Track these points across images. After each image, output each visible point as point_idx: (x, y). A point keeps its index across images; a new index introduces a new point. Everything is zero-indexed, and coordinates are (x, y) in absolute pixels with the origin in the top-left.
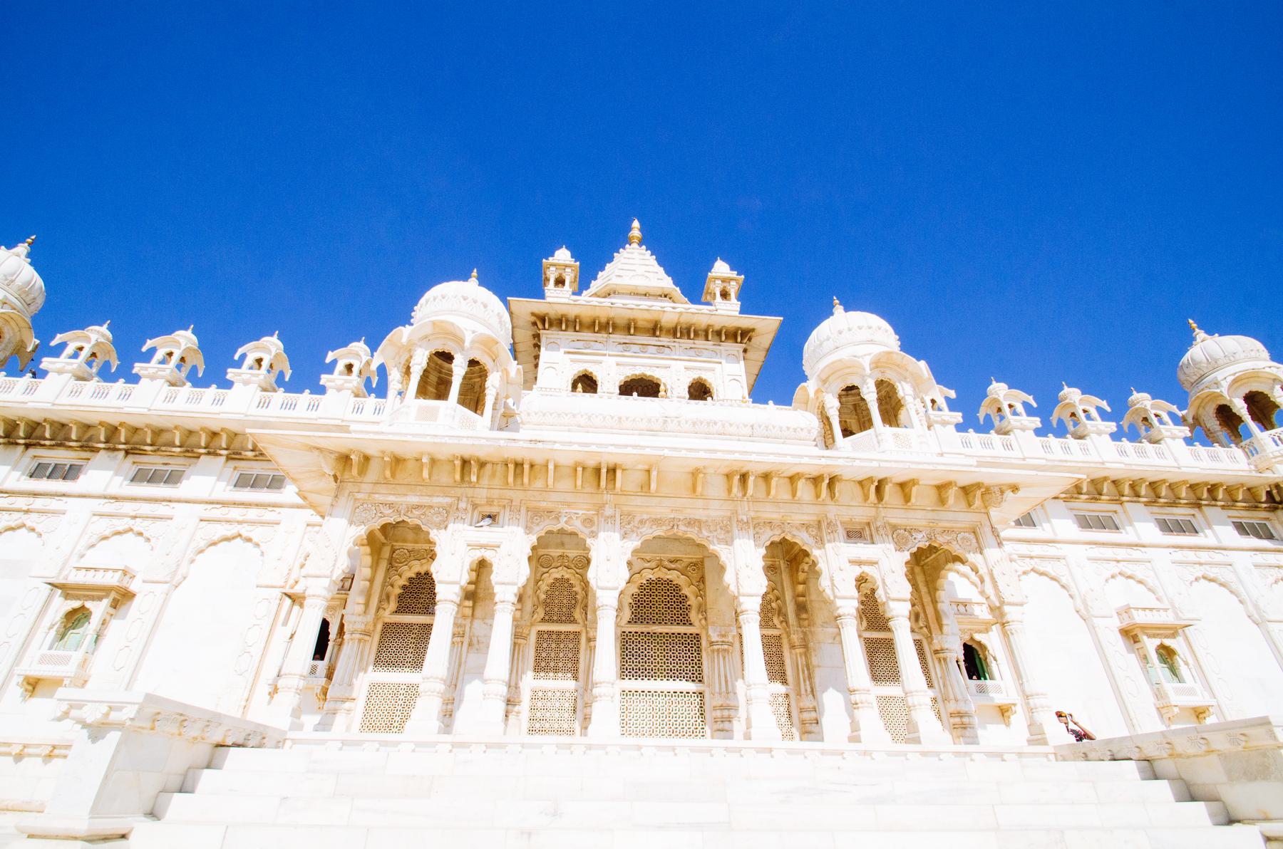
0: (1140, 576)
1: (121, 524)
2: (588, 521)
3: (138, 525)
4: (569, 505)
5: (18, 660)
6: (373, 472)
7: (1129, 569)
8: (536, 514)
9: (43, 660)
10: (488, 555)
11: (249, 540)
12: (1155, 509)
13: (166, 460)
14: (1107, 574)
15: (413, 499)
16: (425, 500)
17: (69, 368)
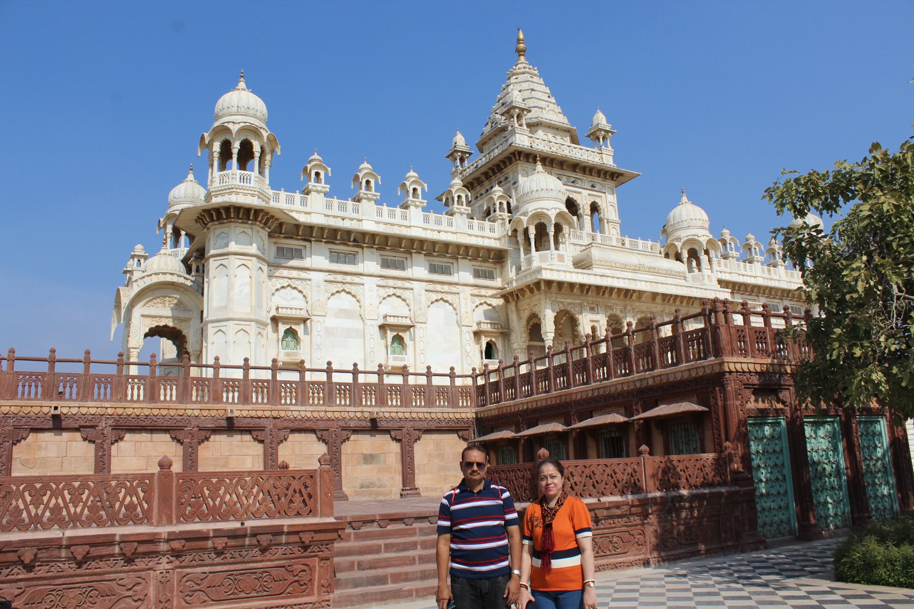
1: (391, 291)
2: (621, 311)
4: (617, 305)
8: (608, 308)
10: (595, 324)
11: (446, 301)
13: (394, 254)
15: (569, 301)
16: (573, 301)
17: (324, 190)
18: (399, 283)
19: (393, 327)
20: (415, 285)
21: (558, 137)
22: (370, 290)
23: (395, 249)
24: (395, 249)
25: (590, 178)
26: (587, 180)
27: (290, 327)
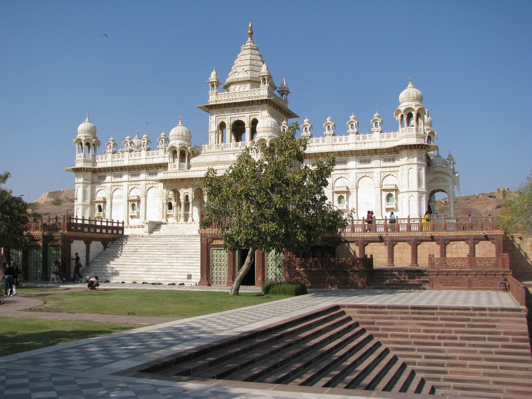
0: (346, 177)
1: (133, 186)
3: (136, 186)
5: (128, 213)
6: (168, 182)
7: (343, 176)
9: (132, 213)
12: (360, 157)
14: (337, 178)
18: (136, 183)
19: (131, 201)
20: (142, 182)
21: (243, 86)
23: (134, 170)
24: (134, 170)
25: (251, 107)
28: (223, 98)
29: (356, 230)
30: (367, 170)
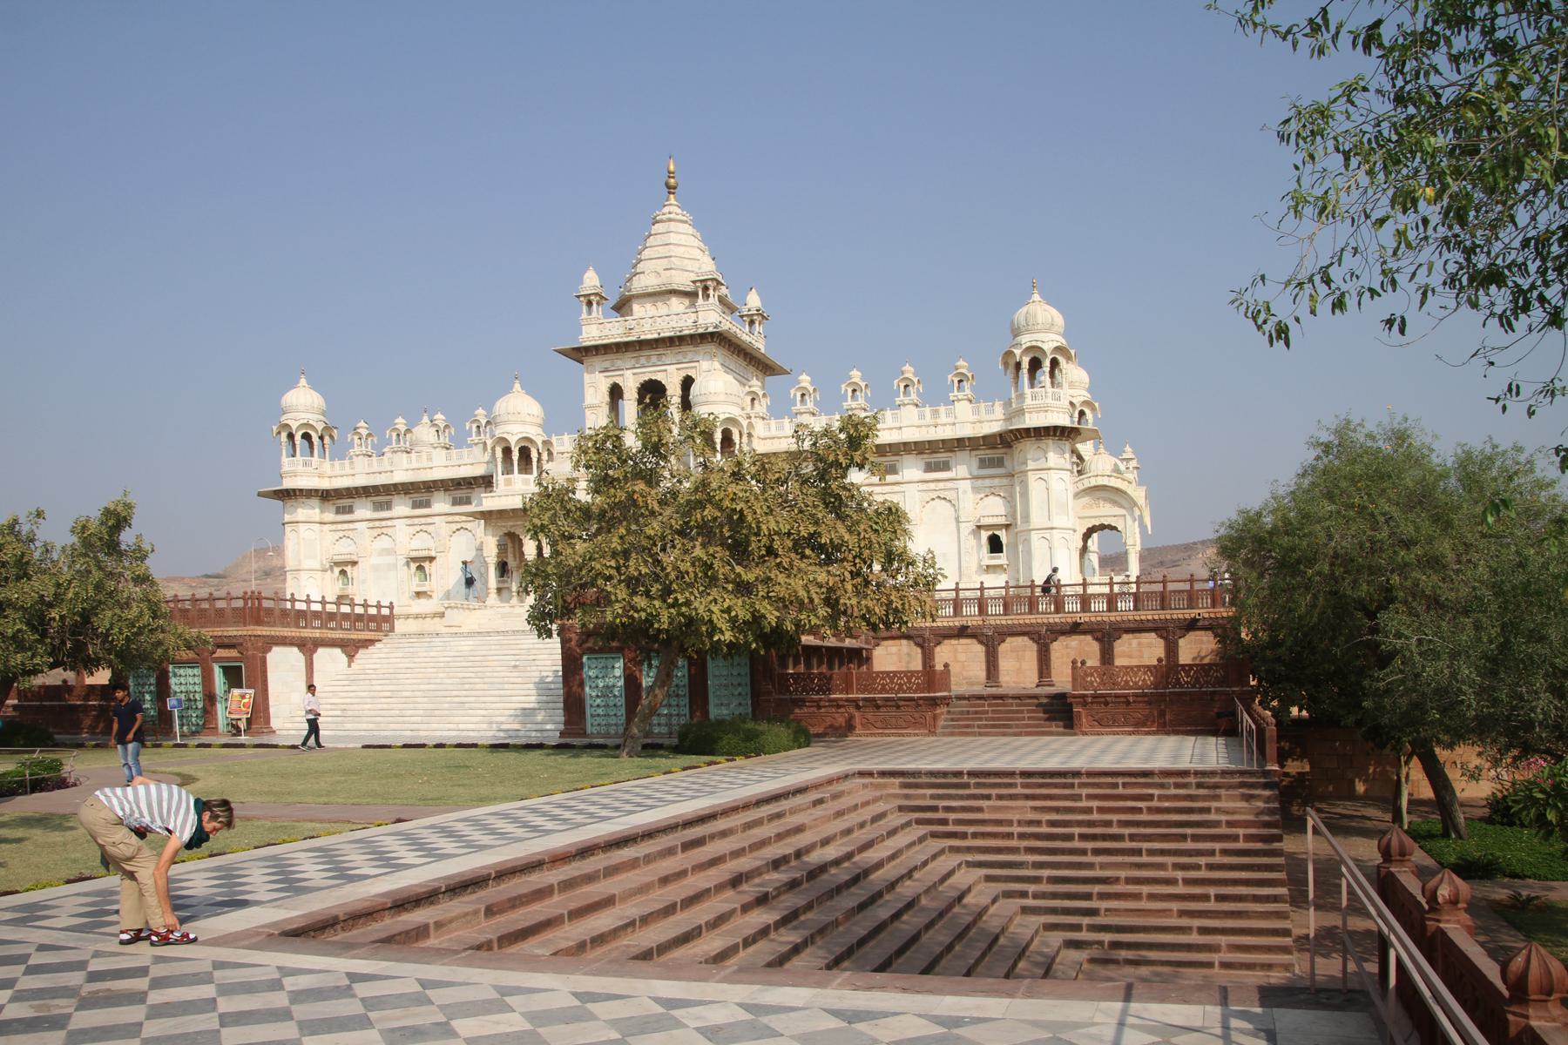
18: (423, 520)
20: (436, 519)
21: (659, 304)
22: (402, 530)
24: (420, 491)
25: (677, 350)
26: (670, 355)
27: (343, 567)
28: (614, 332)
29: (1094, 606)
30: (941, 485)
